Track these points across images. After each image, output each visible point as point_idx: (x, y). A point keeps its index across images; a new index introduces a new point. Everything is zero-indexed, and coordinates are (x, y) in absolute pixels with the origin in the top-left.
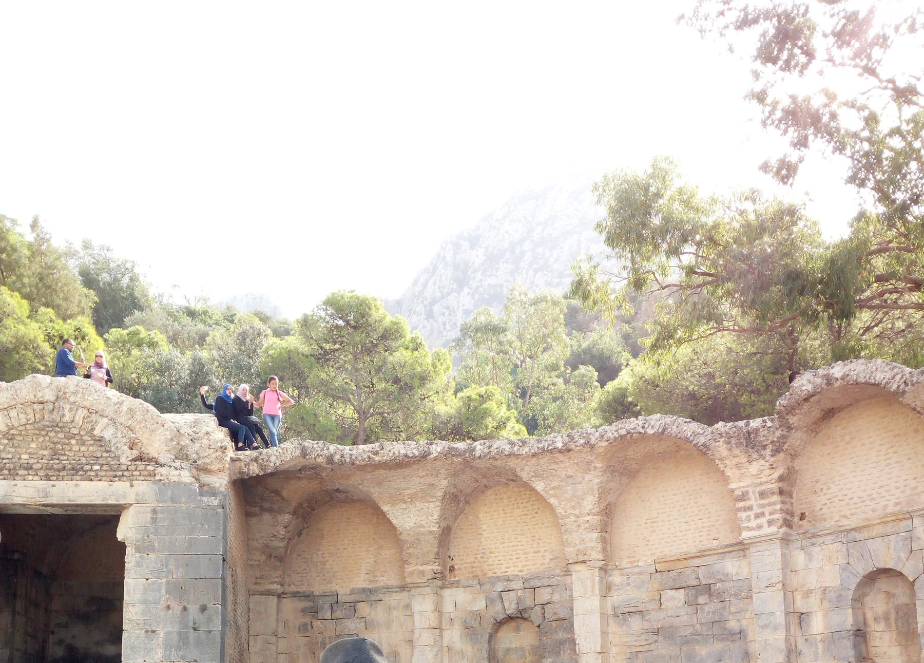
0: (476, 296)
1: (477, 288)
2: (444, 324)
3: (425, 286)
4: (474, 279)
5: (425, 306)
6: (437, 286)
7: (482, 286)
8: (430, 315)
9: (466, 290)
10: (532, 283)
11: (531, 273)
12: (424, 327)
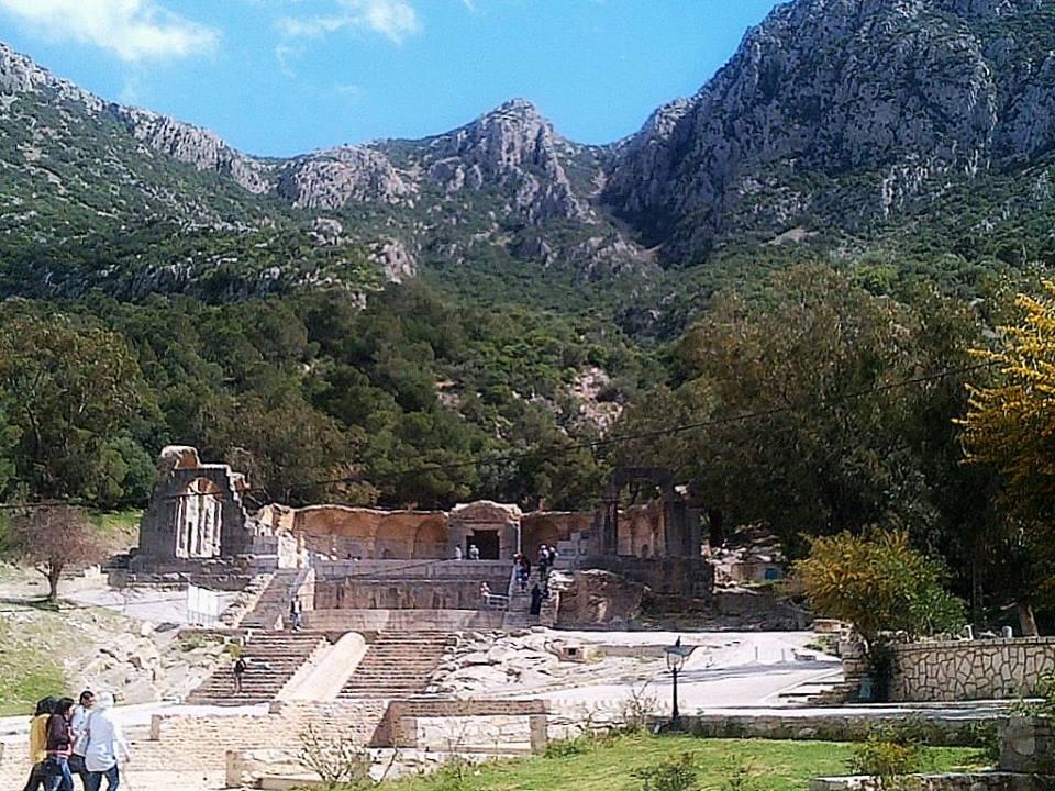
0: (786, 110)
1: (788, 100)
2: (748, 142)
3: (724, 95)
4: (784, 88)
5: (724, 123)
6: (739, 95)
7: (794, 98)
9: (775, 102)
10: (856, 95)
12: (721, 148)
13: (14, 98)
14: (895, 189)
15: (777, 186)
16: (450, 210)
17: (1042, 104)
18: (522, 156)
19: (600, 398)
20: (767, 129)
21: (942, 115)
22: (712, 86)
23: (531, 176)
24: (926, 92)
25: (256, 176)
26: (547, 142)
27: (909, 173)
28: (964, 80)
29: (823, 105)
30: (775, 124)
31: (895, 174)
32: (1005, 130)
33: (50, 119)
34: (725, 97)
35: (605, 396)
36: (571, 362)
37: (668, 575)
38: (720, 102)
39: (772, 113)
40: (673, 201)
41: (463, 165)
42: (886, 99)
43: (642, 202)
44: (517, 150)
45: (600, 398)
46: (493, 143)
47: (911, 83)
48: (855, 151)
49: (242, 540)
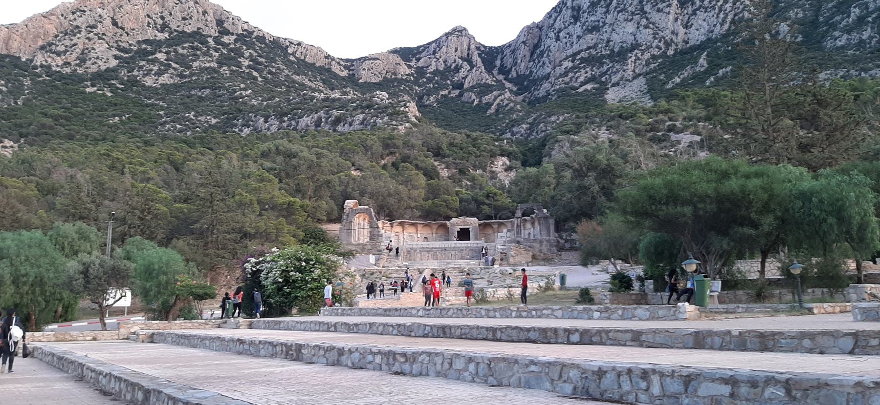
0: (584, 28)
1: (585, 22)
2: (566, 43)
3: (555, 20)
8: (558, 39)
9: (578, 24)
11: (616, 13)
13: (235, 37)
14: (635, 63)
15: (579, 64)
16: (430, 80)
17: (704, 20)
18: (462, 53)
19: (506, 170)
20: (575, 37)
21: (657, 27)
22: (549, 15)
23: (465, 63)
24: (649, 17)
25: (342, 68)
26: (473, 47)
27: (642, 55)
28: (667, 10)
29: (601, 24)
30: (578, 34)
31: (636, 56)
32: (686, 33)
33: (250, 46)
34: (555, 22)
35: (508, 169)
36: (493, 155)
37: (541, 245)
38: (553, 25)
39: (577, 29)
40: (531, 72)
41: (435, 60)
42: (631, 20)
43: (517, 73)
44: (459, 51)
45: (506, 170)
46: (449, 48)
47: (643, 13)
48: (616, 46)
49: (378, 235)
